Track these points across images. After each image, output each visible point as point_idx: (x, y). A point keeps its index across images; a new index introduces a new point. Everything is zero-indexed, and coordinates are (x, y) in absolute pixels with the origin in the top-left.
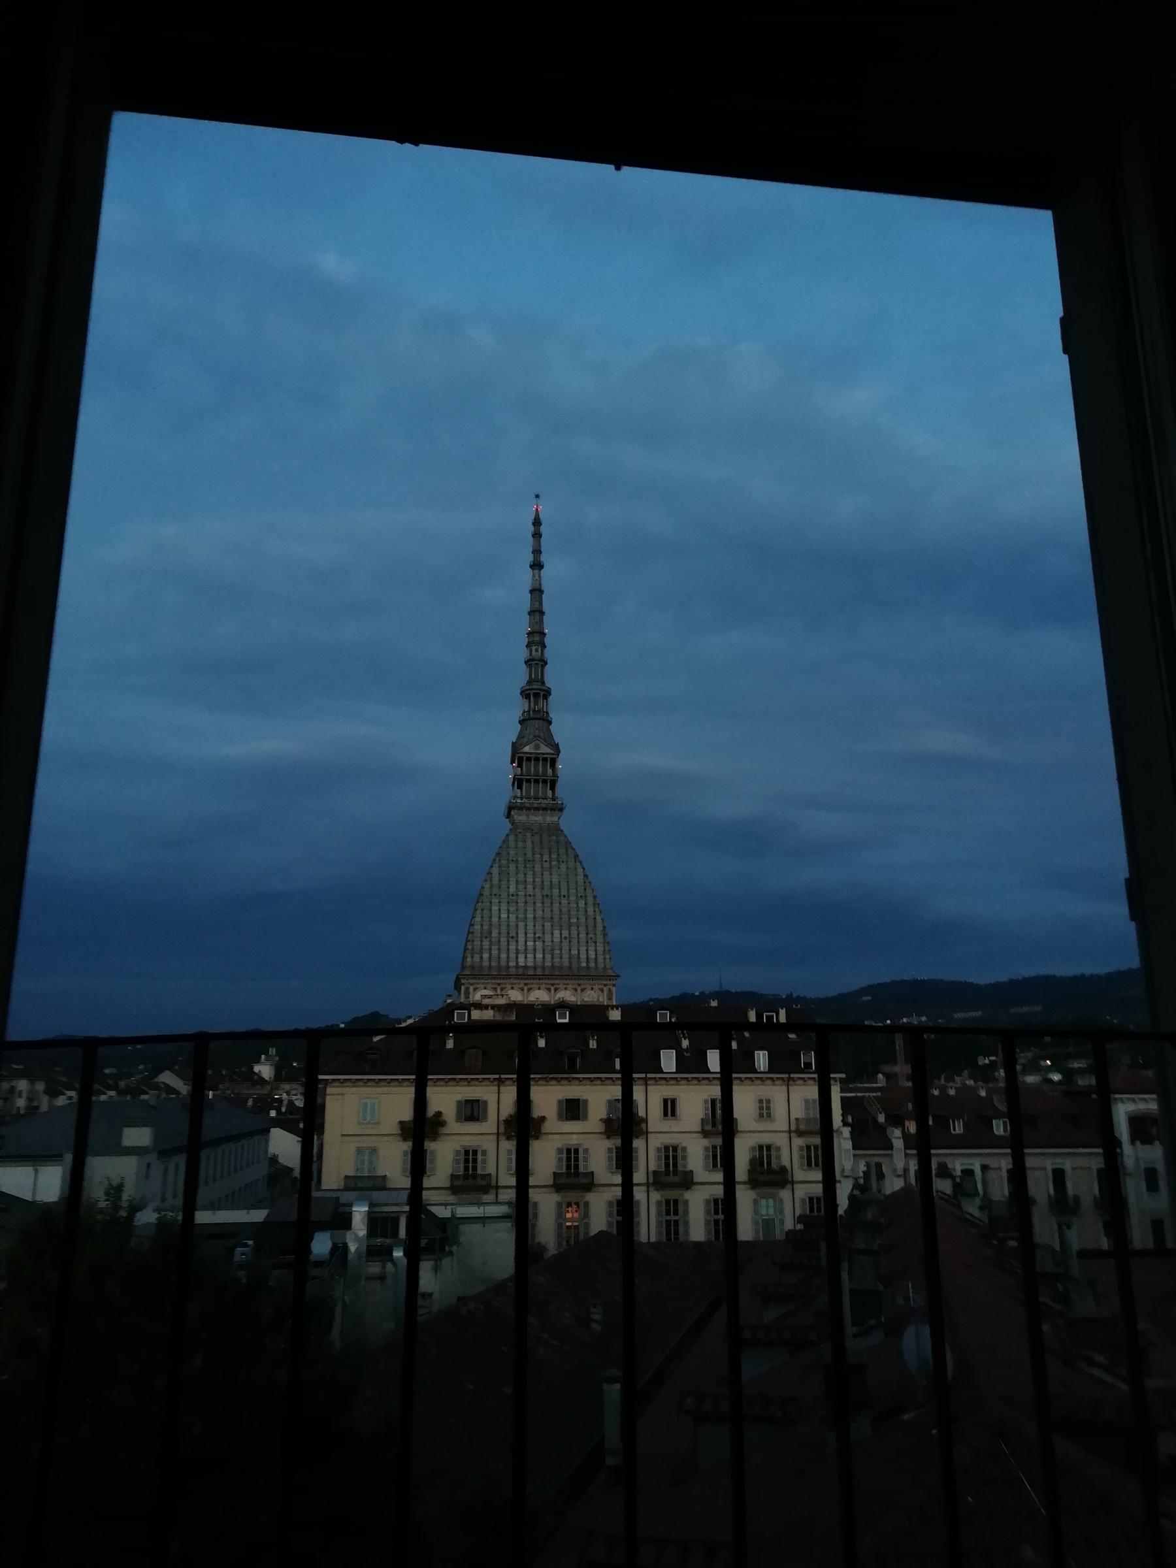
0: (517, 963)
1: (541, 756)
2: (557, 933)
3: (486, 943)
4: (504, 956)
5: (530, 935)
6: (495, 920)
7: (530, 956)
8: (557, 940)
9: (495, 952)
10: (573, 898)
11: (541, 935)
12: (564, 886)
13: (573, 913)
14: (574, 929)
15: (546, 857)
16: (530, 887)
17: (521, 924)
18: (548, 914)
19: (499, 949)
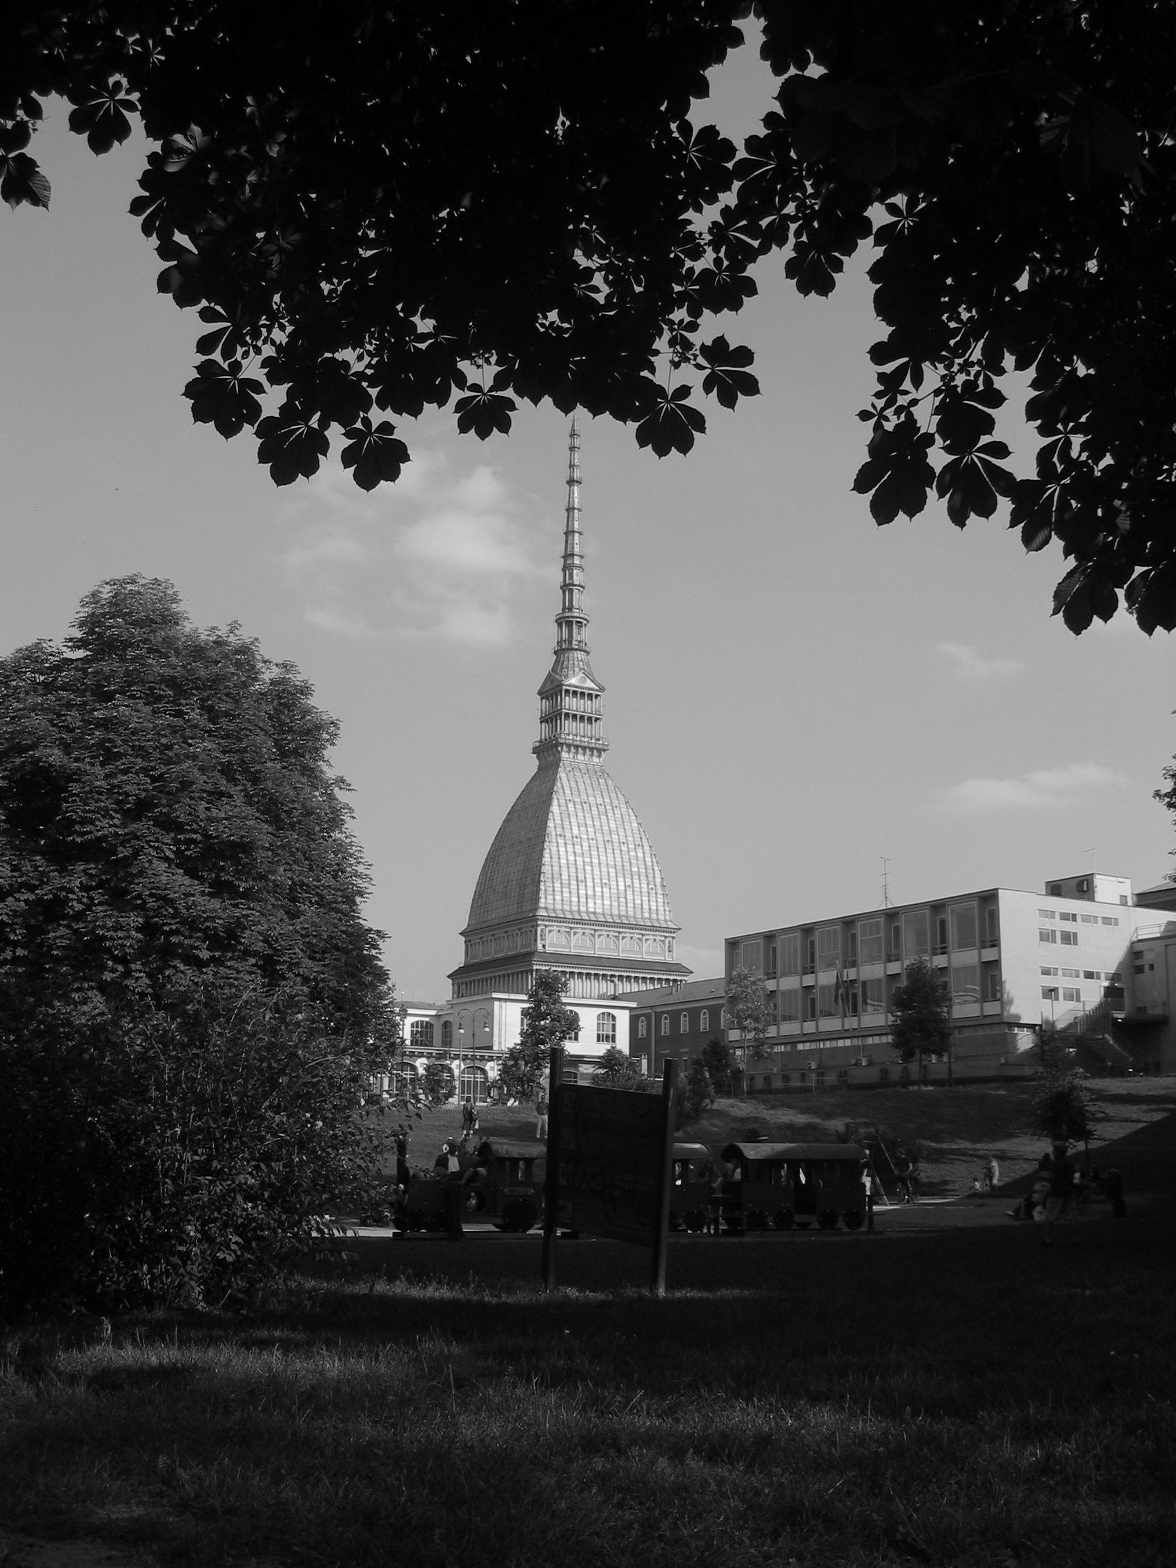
0: (587, 907)
1: (587, 692)
2: (621, 879)
3: (557, 885)
4: (575, 899)
5: (597, 881)
6: (563, 861)
7: (599, 902)
8: (621, 888)
9: (566, 895)
10: (632, 846)
11: (607, 881)
12: (622, 833)
13: (634, 862)
14: (636, 877)
15: (600, 801)
16: (591, 830)
17: (588, 868)
18: (611, 862)
19: (570, 892)
